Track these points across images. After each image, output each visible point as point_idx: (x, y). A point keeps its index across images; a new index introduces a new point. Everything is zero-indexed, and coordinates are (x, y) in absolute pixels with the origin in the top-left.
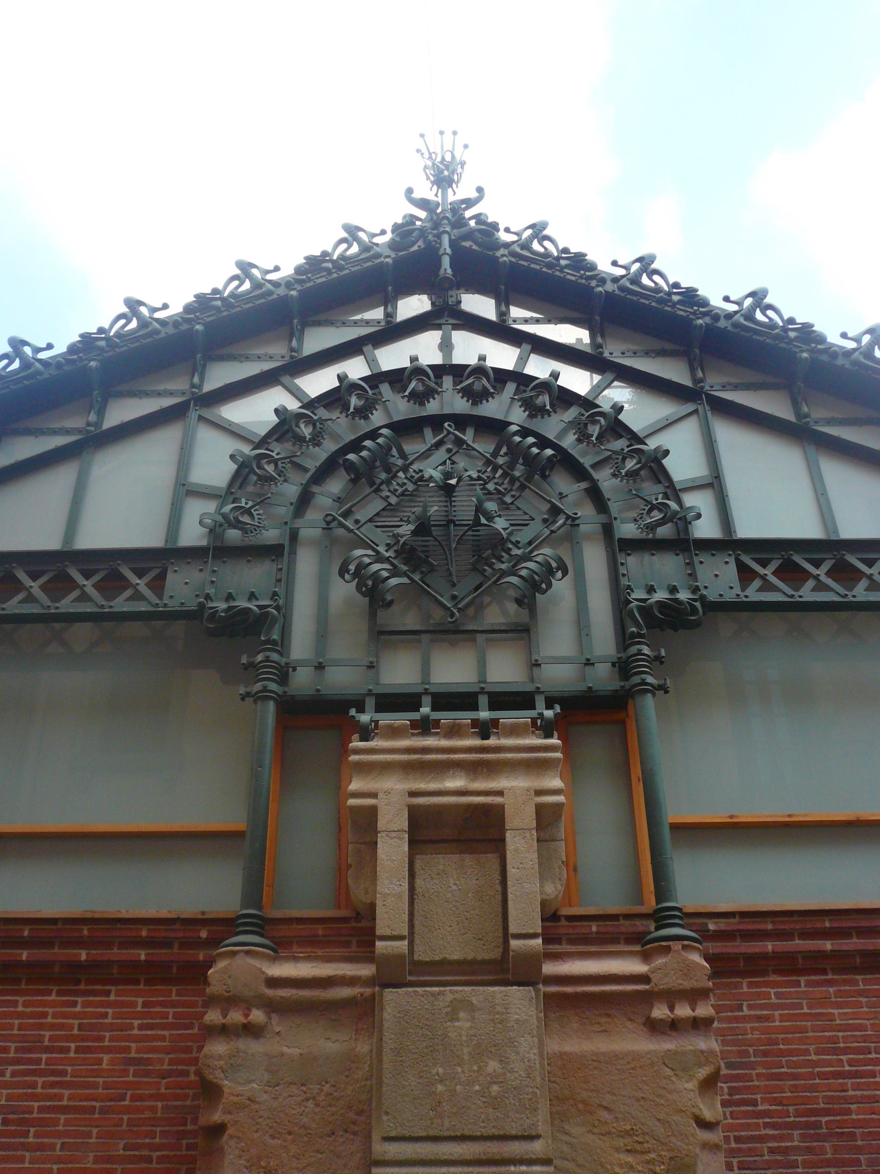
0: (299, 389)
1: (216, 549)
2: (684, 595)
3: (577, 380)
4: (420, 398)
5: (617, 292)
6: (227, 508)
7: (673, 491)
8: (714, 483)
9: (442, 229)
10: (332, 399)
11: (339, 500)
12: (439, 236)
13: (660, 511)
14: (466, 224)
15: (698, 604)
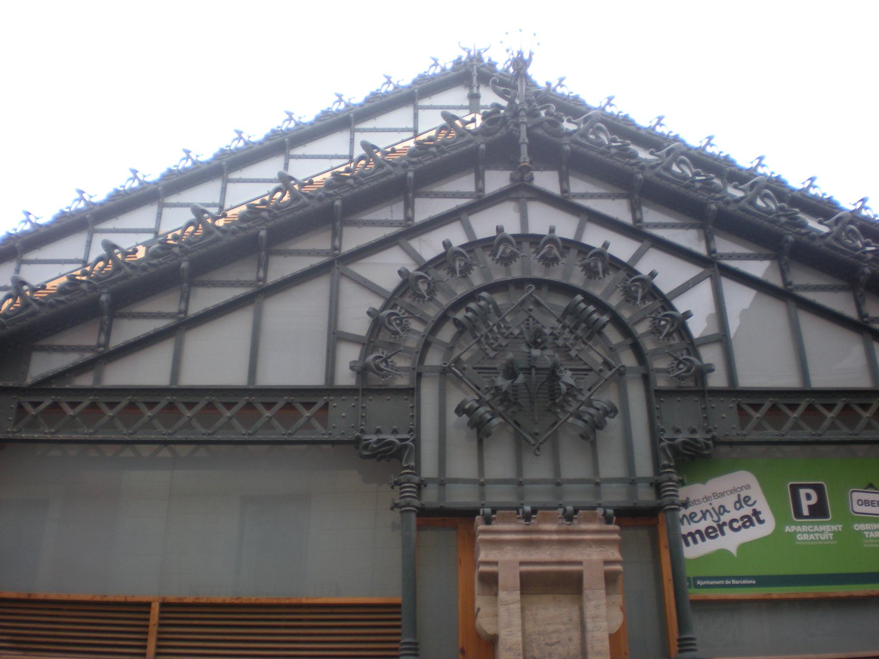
0: (414, 251)
1: (363, 390)
3: (622, 248)
4: (506, 260)
5: (654, 178)
6: (370, 358)
7: (692, 346)
9: (521, 120)
10: (440, 261)
11: (450, 348)
12: (517, 125)
13: (685, 364)
14: (538, 115)
15: (710, 442)
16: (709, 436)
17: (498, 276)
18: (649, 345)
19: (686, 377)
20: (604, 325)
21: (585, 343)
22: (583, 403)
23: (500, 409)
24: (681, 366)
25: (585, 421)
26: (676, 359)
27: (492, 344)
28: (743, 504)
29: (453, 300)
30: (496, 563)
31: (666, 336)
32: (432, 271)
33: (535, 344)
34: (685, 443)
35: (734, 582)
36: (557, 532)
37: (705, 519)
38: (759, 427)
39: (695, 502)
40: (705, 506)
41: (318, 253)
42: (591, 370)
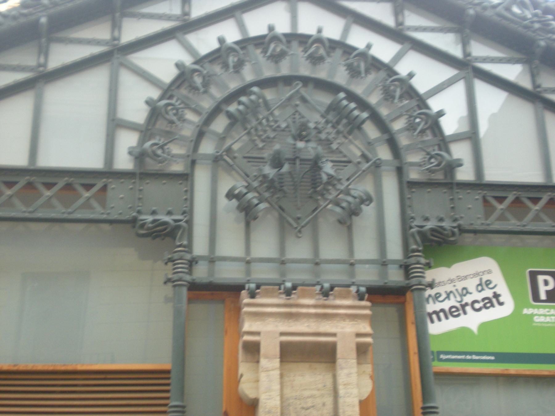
1: (141, 174)
2: (446, 224)
4: (277, 58)
6: (148, 144)
7: (444, 142)
8: (472, 136)
10: (215, 56)
11: (222, 139)
13: (436, 159)
15: (456, 230)
16: (455, 225)
17: (268, 72)
18: (403, 141)
19: (437, 171)
20: (363, 122)
21: (346, 137)
22: (341, 192)
23: (267, 195)
24: (433, 160)
25: (343, 208)
26: (428, 154)
27: (261, 135)
28: (485, 287)
29: (226, 93)
30: (258, 333)
31: (420, 132)
32: (207, 65)
33: (300, 137)
34: (432, 230)
35: (475, 357)
36: (315, 306)
37: (449, 299)
38: (502, 218)
39: (440, 284)
40: (449, 288)
41: (98, 42)
42: (349, 162)
